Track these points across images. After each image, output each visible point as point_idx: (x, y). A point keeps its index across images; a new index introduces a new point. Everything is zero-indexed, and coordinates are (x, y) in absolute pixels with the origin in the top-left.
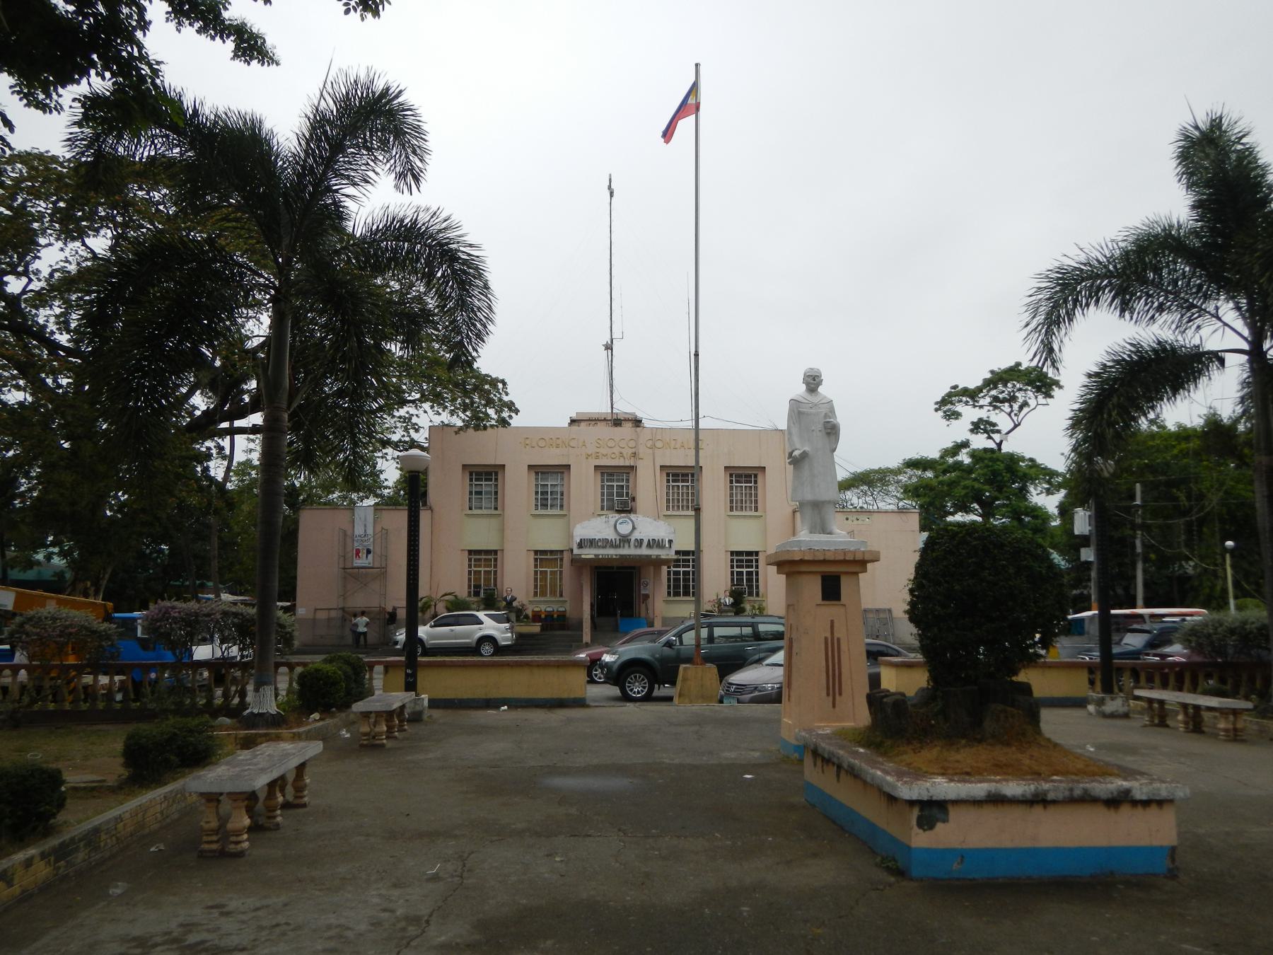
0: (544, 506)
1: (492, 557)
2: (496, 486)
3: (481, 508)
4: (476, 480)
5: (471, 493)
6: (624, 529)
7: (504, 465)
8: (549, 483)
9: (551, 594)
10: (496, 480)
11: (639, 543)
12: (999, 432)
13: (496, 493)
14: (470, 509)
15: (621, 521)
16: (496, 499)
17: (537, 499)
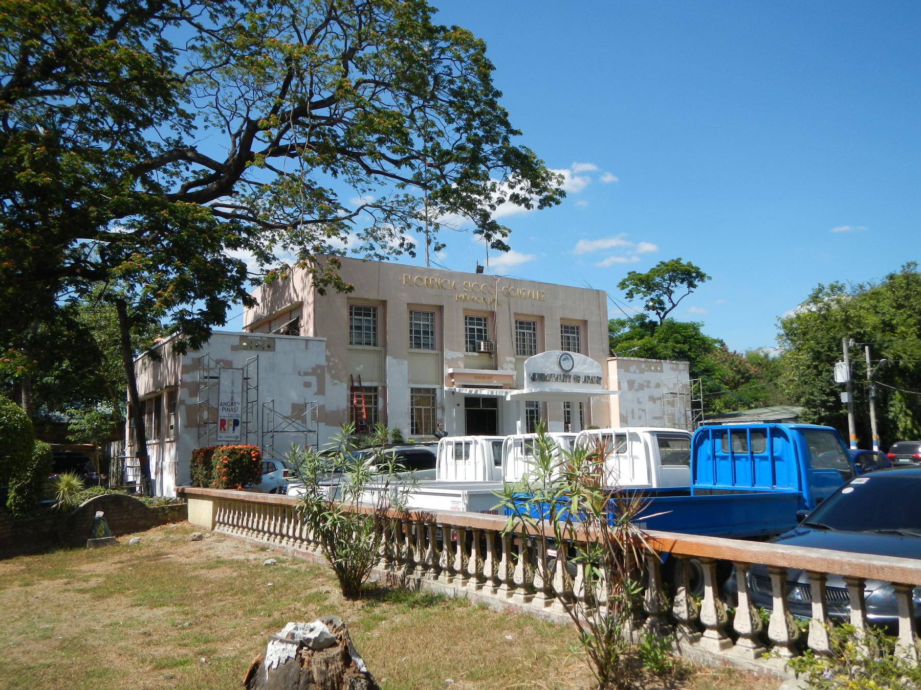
0: (418, 345)
1: (372, 394)
2: (374, 321)
3: (361, 344)
4: (356, 314)
5: (351, 328)
6: (566, 365)
7: (384, 303)
8: (422, 323)
9: (425, 430)
10: (374, 315)
11: (577, 379)
12: (663, 309)
13: (374, 329)
14: (351, 343)
15: (563, 357)
16: (375, 335)
17: (411, 337)
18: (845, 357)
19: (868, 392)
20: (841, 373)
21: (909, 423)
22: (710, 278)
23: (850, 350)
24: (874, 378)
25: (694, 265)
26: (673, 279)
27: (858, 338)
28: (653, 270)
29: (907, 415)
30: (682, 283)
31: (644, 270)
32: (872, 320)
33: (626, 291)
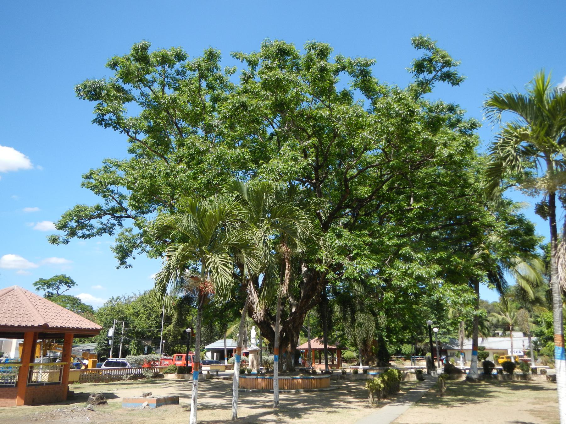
18: (114, 326)
19: (121, 340)
20: (111, 333)
21: (135, 352)
22: (77, 285)
23: (116, 324)
24: (124, 334)
25: (71, 278)
26: (60, 283)
27: (122, 319)
28: (52, 279)
29: (135, 348)
30: (65, 284)
31: (47, 277)
32: (131, 311)
33: (36, 287)
